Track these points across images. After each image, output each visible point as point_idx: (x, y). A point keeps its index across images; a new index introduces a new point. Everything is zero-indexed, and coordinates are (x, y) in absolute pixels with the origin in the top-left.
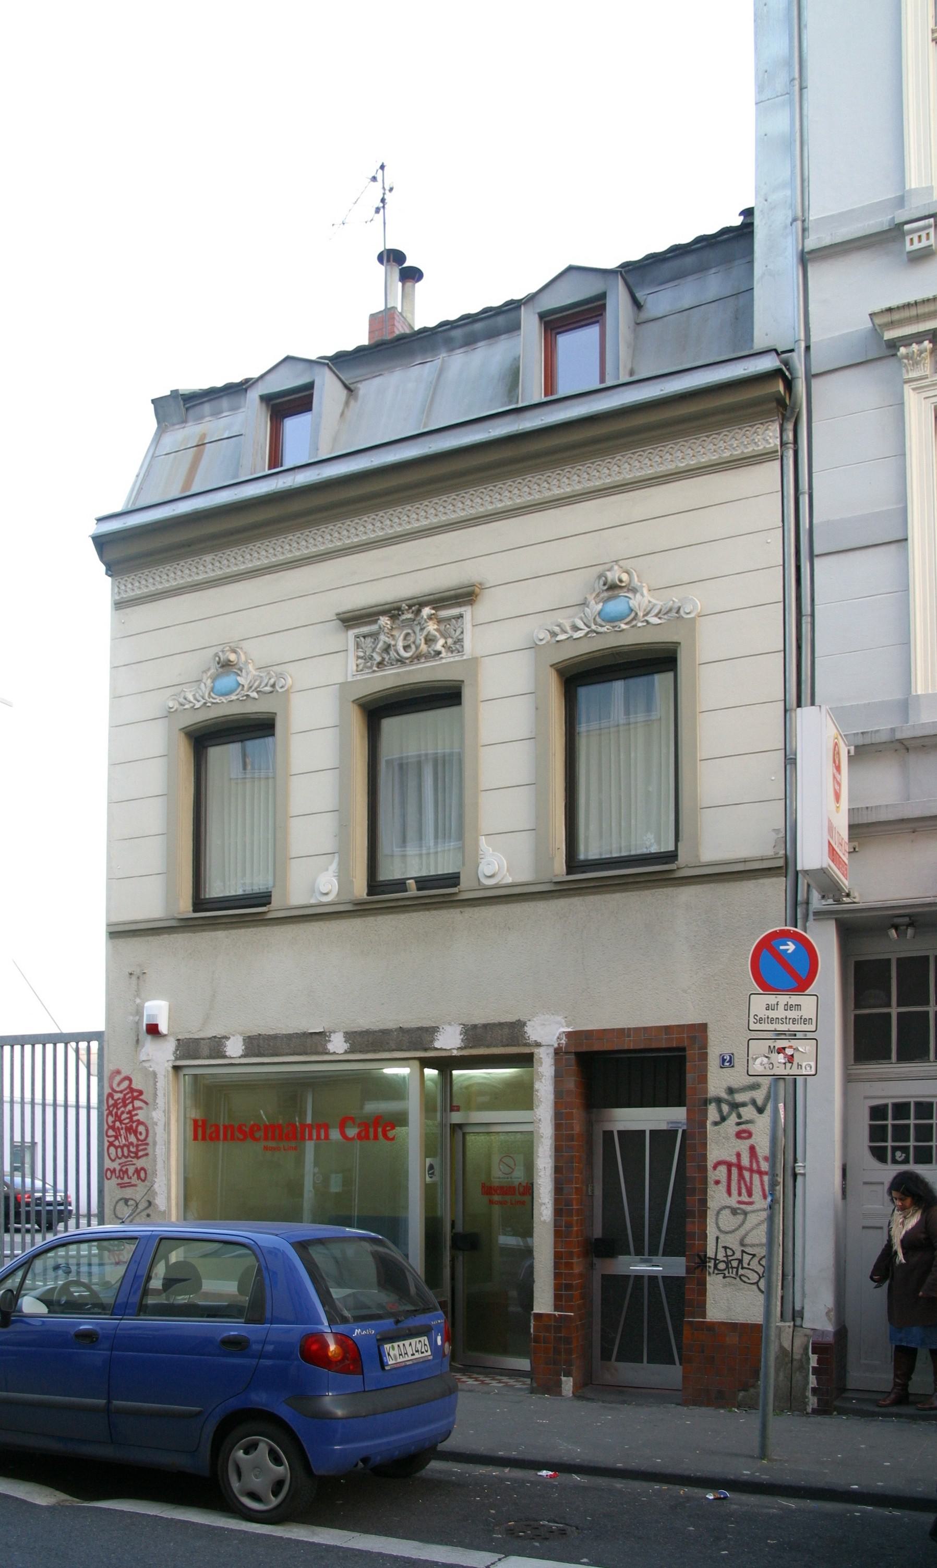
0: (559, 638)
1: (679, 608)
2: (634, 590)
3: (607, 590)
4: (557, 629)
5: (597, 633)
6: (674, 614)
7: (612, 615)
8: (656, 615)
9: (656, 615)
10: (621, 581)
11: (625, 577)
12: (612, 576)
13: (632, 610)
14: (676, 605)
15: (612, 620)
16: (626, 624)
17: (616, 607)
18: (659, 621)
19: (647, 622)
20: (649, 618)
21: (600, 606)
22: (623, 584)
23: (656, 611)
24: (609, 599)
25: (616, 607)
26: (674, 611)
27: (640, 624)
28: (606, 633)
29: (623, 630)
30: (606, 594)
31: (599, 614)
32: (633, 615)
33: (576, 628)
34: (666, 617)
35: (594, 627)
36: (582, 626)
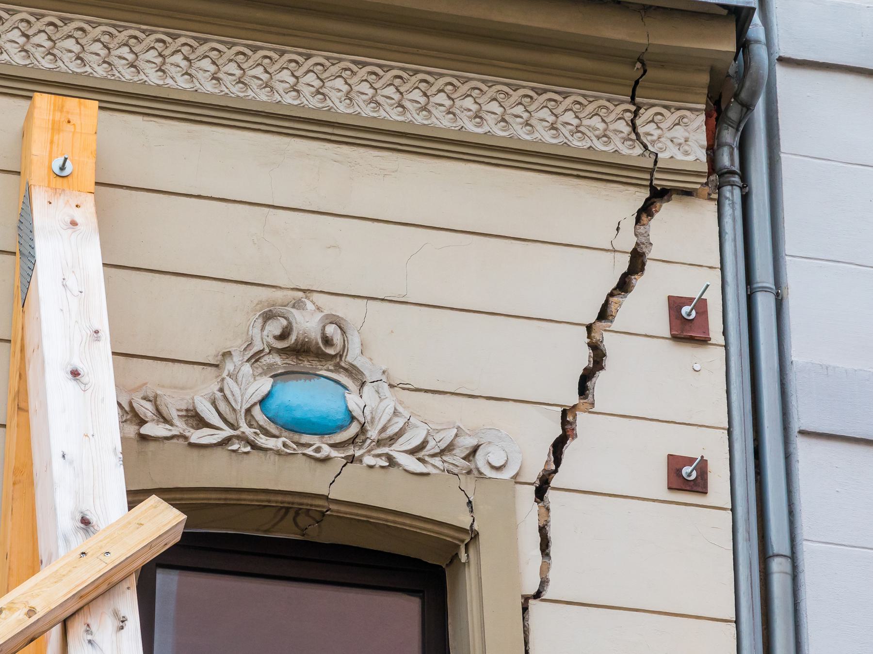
0: (146, 430)
1: (475, 450)
2: (353, 372)
3: (281, 352)
4: (146, 409)
5: (255, 447)
6: (456, 459)
7: (298, 414)
8: (413, 452)
9: (413, 452)
10: (327, 341)
11: (331, 330)
12: (307, 324)
13: (353, 418)
14: (468, 442)
15: (296, 427)
16: (333, 446)
17: (308, 396)
18: (420, 468)
19: (390, 459)
20: (396, 451)
21: (265, 385)
22: (331, 351)
23: (413, 439)
24: (288, 374)
25: (308, 396)
26: (460, 452)
27: (369, 460)
28: (278, 453)
29: (326, 460)
30: (276, 359)
31: (262, 402)
32: (354, 429)
33: (200, 422)
34: (437, 461)
35: (244, 428)
36: (212, 417)
